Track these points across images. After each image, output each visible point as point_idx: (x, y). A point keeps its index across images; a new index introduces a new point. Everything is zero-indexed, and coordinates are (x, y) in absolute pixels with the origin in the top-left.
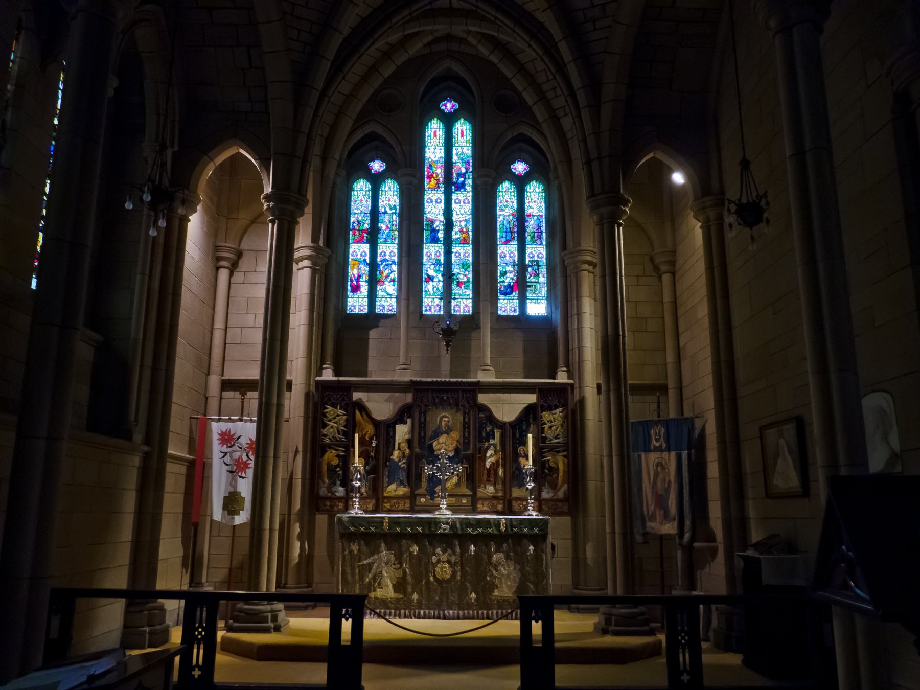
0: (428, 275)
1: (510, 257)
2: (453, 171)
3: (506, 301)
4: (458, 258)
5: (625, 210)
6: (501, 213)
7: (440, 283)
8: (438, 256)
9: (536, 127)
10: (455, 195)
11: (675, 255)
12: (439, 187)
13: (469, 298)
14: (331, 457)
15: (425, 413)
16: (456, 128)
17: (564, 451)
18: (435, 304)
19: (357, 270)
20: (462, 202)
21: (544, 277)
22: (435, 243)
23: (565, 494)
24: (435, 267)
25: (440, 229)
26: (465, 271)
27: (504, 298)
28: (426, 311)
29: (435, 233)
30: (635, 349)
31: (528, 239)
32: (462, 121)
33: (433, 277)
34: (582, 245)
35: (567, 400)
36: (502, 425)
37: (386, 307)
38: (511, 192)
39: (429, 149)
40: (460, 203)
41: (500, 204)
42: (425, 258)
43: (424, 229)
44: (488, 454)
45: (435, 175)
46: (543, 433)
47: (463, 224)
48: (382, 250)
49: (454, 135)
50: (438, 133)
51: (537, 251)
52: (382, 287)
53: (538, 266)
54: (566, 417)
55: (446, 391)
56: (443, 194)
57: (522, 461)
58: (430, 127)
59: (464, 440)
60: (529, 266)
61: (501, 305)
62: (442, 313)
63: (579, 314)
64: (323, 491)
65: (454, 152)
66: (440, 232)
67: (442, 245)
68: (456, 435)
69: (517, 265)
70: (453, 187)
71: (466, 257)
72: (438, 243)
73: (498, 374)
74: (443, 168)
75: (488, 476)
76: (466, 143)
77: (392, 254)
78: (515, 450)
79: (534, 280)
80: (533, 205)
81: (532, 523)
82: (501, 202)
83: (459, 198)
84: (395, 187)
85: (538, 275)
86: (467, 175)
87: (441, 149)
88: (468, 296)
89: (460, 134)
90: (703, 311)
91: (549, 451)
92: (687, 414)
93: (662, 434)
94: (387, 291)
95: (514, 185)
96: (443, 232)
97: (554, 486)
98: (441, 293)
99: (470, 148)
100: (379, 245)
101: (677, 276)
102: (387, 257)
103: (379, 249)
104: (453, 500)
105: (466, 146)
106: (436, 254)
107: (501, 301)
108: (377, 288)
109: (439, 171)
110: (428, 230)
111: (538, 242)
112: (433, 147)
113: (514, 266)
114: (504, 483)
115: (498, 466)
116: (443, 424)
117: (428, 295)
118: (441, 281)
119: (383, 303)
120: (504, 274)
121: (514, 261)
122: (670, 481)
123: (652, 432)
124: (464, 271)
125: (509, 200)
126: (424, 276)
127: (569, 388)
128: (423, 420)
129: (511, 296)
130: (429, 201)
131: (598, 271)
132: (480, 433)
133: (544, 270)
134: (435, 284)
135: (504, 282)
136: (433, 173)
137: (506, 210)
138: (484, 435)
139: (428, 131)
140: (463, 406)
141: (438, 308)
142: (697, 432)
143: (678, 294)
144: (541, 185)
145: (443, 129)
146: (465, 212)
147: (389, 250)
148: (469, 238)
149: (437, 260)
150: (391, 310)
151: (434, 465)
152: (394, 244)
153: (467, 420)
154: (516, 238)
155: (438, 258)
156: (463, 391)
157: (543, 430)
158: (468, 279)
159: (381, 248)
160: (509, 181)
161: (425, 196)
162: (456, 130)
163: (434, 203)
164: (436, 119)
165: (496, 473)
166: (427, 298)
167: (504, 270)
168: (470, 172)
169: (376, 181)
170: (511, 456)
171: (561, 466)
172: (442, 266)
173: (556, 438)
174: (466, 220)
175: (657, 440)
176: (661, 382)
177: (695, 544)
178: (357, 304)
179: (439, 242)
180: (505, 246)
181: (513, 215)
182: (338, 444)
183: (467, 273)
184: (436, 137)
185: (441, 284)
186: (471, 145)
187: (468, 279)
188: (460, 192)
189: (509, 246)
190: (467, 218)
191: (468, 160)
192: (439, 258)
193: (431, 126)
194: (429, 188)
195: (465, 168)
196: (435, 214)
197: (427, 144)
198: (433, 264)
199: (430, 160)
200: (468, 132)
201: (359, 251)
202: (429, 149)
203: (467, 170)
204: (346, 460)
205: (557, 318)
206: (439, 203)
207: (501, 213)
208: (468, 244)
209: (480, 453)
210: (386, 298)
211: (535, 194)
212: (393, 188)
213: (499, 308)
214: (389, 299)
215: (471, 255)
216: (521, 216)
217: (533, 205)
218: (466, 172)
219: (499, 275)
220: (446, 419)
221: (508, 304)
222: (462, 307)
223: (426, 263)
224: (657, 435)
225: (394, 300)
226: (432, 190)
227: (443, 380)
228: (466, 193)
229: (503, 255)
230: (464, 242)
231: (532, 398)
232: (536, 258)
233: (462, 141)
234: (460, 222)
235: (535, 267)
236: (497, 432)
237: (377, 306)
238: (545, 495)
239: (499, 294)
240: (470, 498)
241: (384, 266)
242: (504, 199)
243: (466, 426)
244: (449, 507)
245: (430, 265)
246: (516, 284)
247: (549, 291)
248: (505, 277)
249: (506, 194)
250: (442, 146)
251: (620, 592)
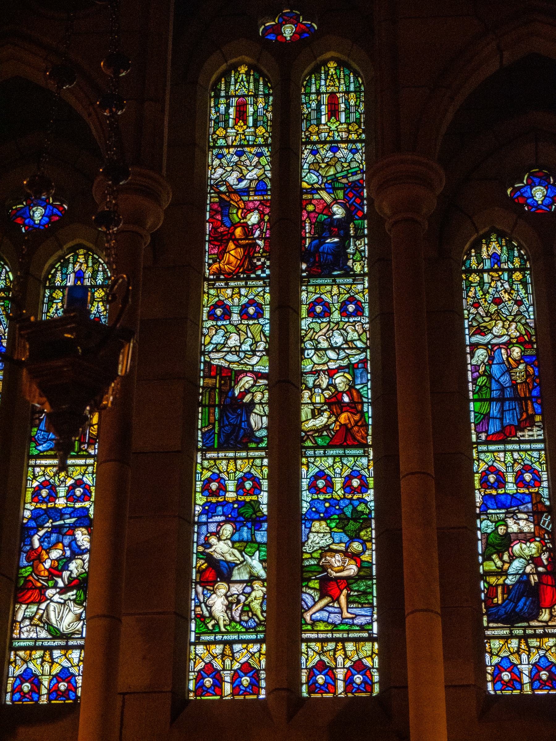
0: (209, 558)
1: (519, 481)
3: (514, 643)
4: (322, 497)
6: (477, 339)
7: (257, 585)
8: (248, 493)
10: (311, 289)
12: (254, 268)
13: (371, 639)
16: (313, 90)
18: (236, 666)
22: (235, 449)
24: (236, 530)
25: (257, 400)
26: (352, 540)
27: (506, 632)
28: (200, 689)
29: (241, 415)
32: (332, 71)
33: (231, 566)
37: (46, 683)
38: (511, 272)
39: (220, 156)
40: (327, 312)
41: (473, 310)
42: (200, 499)
43: (200, 404)
45: (238, 232)
47: (340, 380)
48: (42, 479)
49: (305, 111)
50: (250, 110)
52: (34, 608)
56: (267, 289)
58: (223, 94)
61: (496, 660)
62: (262, 697)
65: (308, 158)
66: (258, 409)
67: (263, 454)
69: (549, 510)
70: (304, 266)
71: (353, 490)
72: (248, 449)
74: (267, 211)
76: (349, 132)
77: (78, 492)
82: (476, 305)
83: (327, 298)
84: (100, 276)
86: (352, 225)
87: (259, 155)
88: (362, 628)
94: (53, 621)
95: (520, 247)
96: (266, 408)
98: (258, 625)
99: (359, 145)
100: (32, 462)
102: (61, 503)
103: (30, 477)
105: (347, 141)
106: (240, 486)
107: (496, 644)
108: (15, 613)
109: (253, 218)
110: (212, 406)
112: (232, 150)
117: (211, 632)
118: (258, 578)
119: (35, 667)
124: (346, 539)
125: (506, 296)
126: (197, 563)
129: (533, 623)
130: (219, 312)
134: (236, 589)
135: (502, 573)
136: (235, 226)
139: (216, 106)
141: (246, 681)
145: (266, 96)
146: (346, 342)
148: (368, 425)
149: (243, 504)
150: (65, 694)
152: (89, 456)
154: (538, 418)
155: (248, 499)
160: (501, 235)
161: (206, 298)
162: (313, 97)
163: (235, 318)
164: (243, 69)
166: (207, 643)
167: (501, 530)
168: (363, 218)
172: (265, 525)
174: (351, 368)
179: (253, 445)
180: (501, 447)
181: (520, 341)
183: (356, 546)
184: (245, 122)
185: (259, 591)
186: (363, 136)
188: (329, 281)
189: (516, 447)
190: (354, 360)
191: (353, 182)
192: (254, 498)
193: (227, 91)
194: (220, 271)
195: (343, 205)
196: (237, 353)
197: (215, 141)
198: (226, 522)
199: (223, 189)
200: (352, 102)
202: (220, 156)
206: (250, 317)
207: (477, 339)
208: (364, 446)
210: (50, 649)
212: (94, 276)
213: (489, 670)
214: (56, 653)
215: (371, 482)
218: (350, 216)
221: (524, 657)
222: (340, 674)
223: (204, 518)
225: (75, 655)
226: (226, 280)
228: (350, 280)
229: (492, 478)
233: (333, 127)
234: (331, 373)
237: (10, 681)
239: (485, 619)
241: (47, 536)
242: (485, 293)
245: (219, 524)
246: (549, 580)
248: (506, 557)
250: (266, 145)
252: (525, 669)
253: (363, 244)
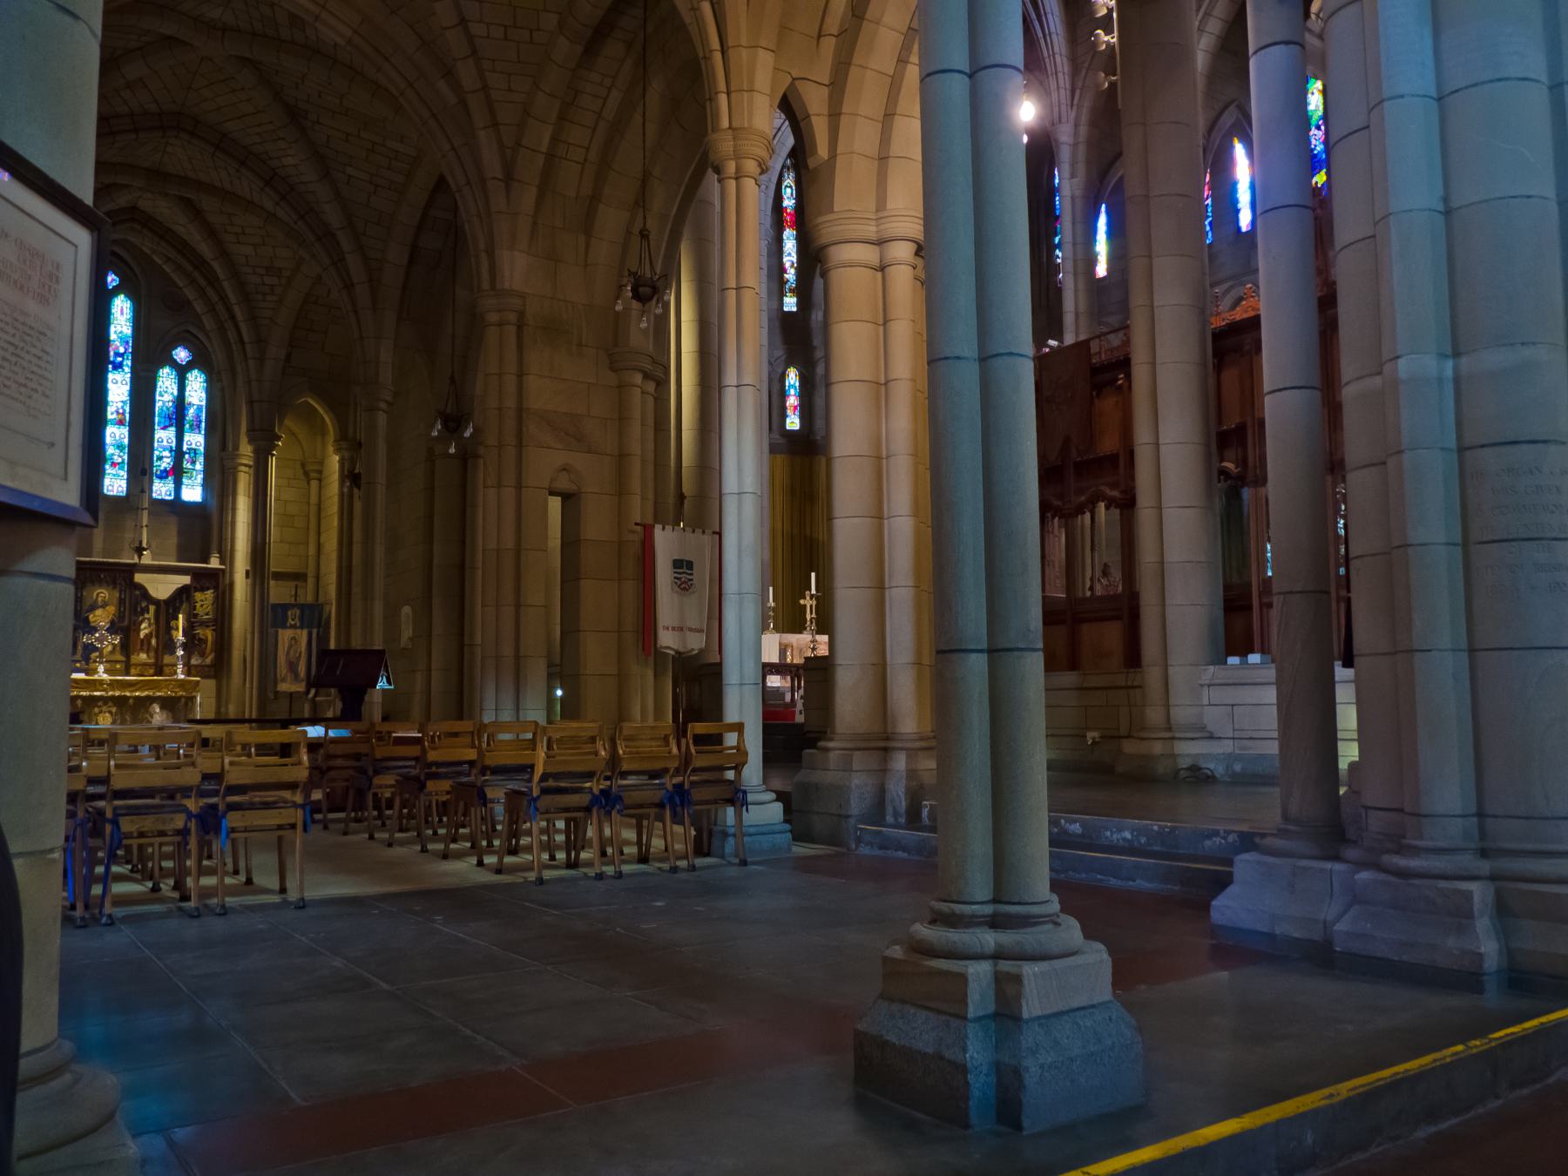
1: (168, 442)
2: (111, 349)
3: (161, 484)
5: (278, 445)
6: (161, 398)
9: (202, 328)
11: (322, 466)
15: (82, 589)
17: (213, 625)
20: (119, 382)
21: (200, 463)
23: (212, 661)
30: (281, 542)
31: (187, 426)
34: (241, 449)
35: (218, 584)
36: (157, 602)
40: (117, 382)
44: (143, 626)
46: (195, 609)
47: (120, 405)
51: (195, 440)
53: (195, 453)
54: (216, 598)
55: (105, 570)
57: (174, 633)
59: (120, 616)
60: (187, 453)
63: (234, 510)
68: (112, 609)
70: (110, 366)
73: (154, 556)
75: (142, 646)
78: (168, 623)
79: (191, 467)
80: (193, 394)
81: (182, 684)
85: (193, 462)
89: (119, 312)
90: (335, 522)
91: (199, 626)
92: (320, 601)
93: (297, 615)
97: (203, 655)
101: (322, 484)
104: (108, 665)
111: (197, 431)
113: (171, 451)
114: (157, 651)
115: (151, 637)
116: (100, 599)
120: (160, 458)
121: (171, 447)
122: (301, 652)
123: (289, 613)
127: (221, 573)
128: (79, 595)
131: (252, 471)
132: (136, 609)
133: (201, 459)
137: (166, 395)
138: (139, 609)
140: (120, 584)
142: (324, 617)
143: (322, 499)
144: (203, 376)
151: (92, 635)
153: (123, 596)
156: (123, 571)
157: (195, 608)
158: (123, 460)
160: (170, 366)
165: (149, 643)
171: (210, 638)
173: (207, 614)
175: (293, 620)
176: (302, 571)
177: (318, 699)
183: (121, 454)
187: (123, 460)
203: (126, 350)
205: (213, 504)
207: (161, 398)
208: (124, 425)
209: (134, 625)
215: (127, 436)
216: (180, 403)
217: (193, 394)
218: (125, 352)
219: (155, 459)
220: (103, 595)
224: (293, 616)
227: (97, 559)
230: (121, 423)
231: (186, 580)
232: (194, 446)
235: (192, 455)
236: (152, 608)
238: (194, 661)
240: (124, 665)
243: (121, 602)
244: (106, 671)
247: (204, 479)
249: (166, 382)
251: (254, 716)
252: (164, 490)
253: (129, 363)
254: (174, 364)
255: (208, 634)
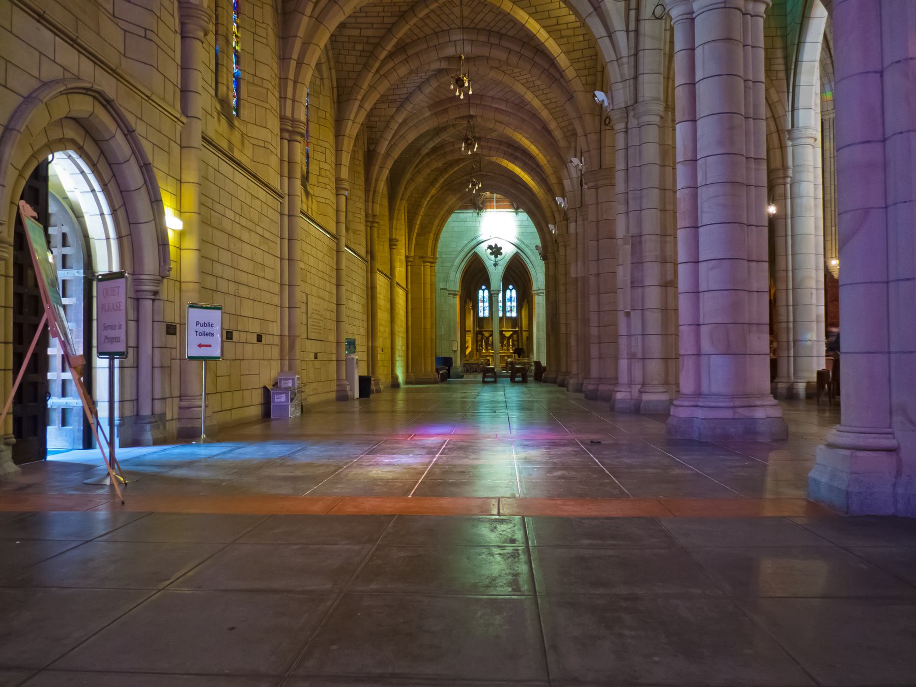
14: (479, 343)
19: (481, 309)
51: (514, 304)
64: (478, 348)
147: (487, 304)
159: (485, 304)
169: (483, 290)
170: (508, 342)
178: (481, 315)
182: (480, 341)
201: (481, 304)
204: (482, 344)
211: (514, 292)
230: (501, 302)
231: (512, 332)
249: (508, 292)
254: (509, 289)
255: (516, 343)
